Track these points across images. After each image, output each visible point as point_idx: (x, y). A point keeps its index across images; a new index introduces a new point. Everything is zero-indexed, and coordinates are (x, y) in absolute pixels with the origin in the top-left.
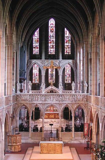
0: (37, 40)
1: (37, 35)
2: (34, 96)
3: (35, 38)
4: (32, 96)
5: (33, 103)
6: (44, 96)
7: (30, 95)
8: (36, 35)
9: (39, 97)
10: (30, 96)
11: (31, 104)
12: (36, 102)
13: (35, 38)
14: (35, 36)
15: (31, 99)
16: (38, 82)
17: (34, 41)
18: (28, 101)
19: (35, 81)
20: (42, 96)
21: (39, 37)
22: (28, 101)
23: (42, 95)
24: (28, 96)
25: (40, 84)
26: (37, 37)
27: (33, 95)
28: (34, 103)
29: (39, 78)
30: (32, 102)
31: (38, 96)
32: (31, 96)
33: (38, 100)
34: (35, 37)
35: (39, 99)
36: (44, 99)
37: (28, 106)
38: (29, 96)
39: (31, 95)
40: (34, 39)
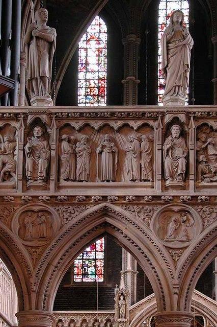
0: (98, 88)
1: (99, 64)
2: (82, 137)
3: (86, 80)
4: (53, 132)
5: (63, 193)
6: (183, 134)
7: (37, 122)
8: (93, 45)
9: (127, 142)
10: (37, 130)
11: (37, 211)
12: (95, 193)
13: (86, 80)
14: (87, 71)
15: (42, 164)
16: (102, 280)
17: (82, 92)
18: (16, 178)
19: (85, 274)
20: (166, 133)
21: (110, 71)
22: (16, 178)
23: (168, 118)
24: (20, 135)
25: (109, 285)
26: (96, 76)
27: (65, 127)
28: (81, 193)
29: (107, 259)
30: (58, 187)
31: (120, 138)
32: (45, 136)
33: (117, 172)
34: (89, 76)
35: (130, 163)
36: (182, 163)
37: (16, 225)
38: (29, 134)
39: (44, 126)
40: (82, 83)
